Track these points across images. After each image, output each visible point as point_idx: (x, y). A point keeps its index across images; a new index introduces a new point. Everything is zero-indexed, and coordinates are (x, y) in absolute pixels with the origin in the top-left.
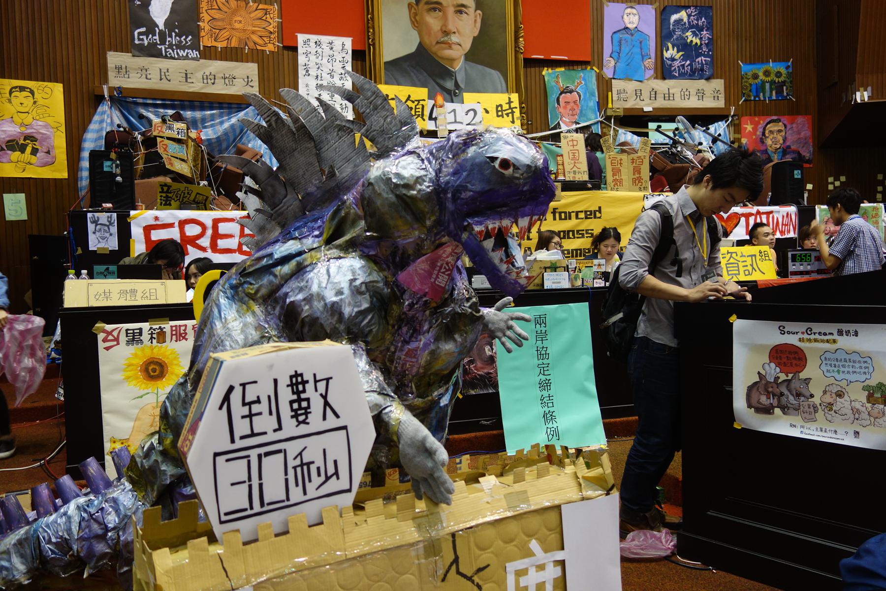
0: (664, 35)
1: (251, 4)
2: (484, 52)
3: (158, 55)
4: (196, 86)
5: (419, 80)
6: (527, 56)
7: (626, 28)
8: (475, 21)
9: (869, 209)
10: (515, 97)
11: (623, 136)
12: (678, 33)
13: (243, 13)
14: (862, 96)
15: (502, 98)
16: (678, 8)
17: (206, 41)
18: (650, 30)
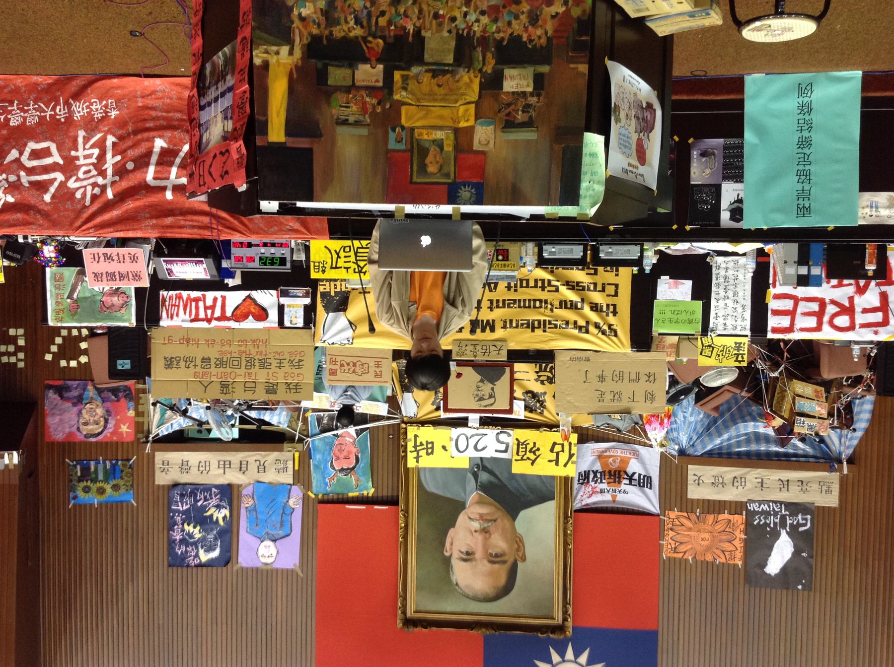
0: (227, 536)
1: (690, 558)
3: (790, 506)
4: (753, 475)
5: (517, 481)
6: (393, 508)
7: (274, 541)
8: (452, 544)
9: (67, 319)
10: (411, 463)
11: (282, 421)
12: (211, 537)
13: (699, 548)
15: (426, 462)
16: (210, 564)
17: (739, 519)
18: (245, 538)
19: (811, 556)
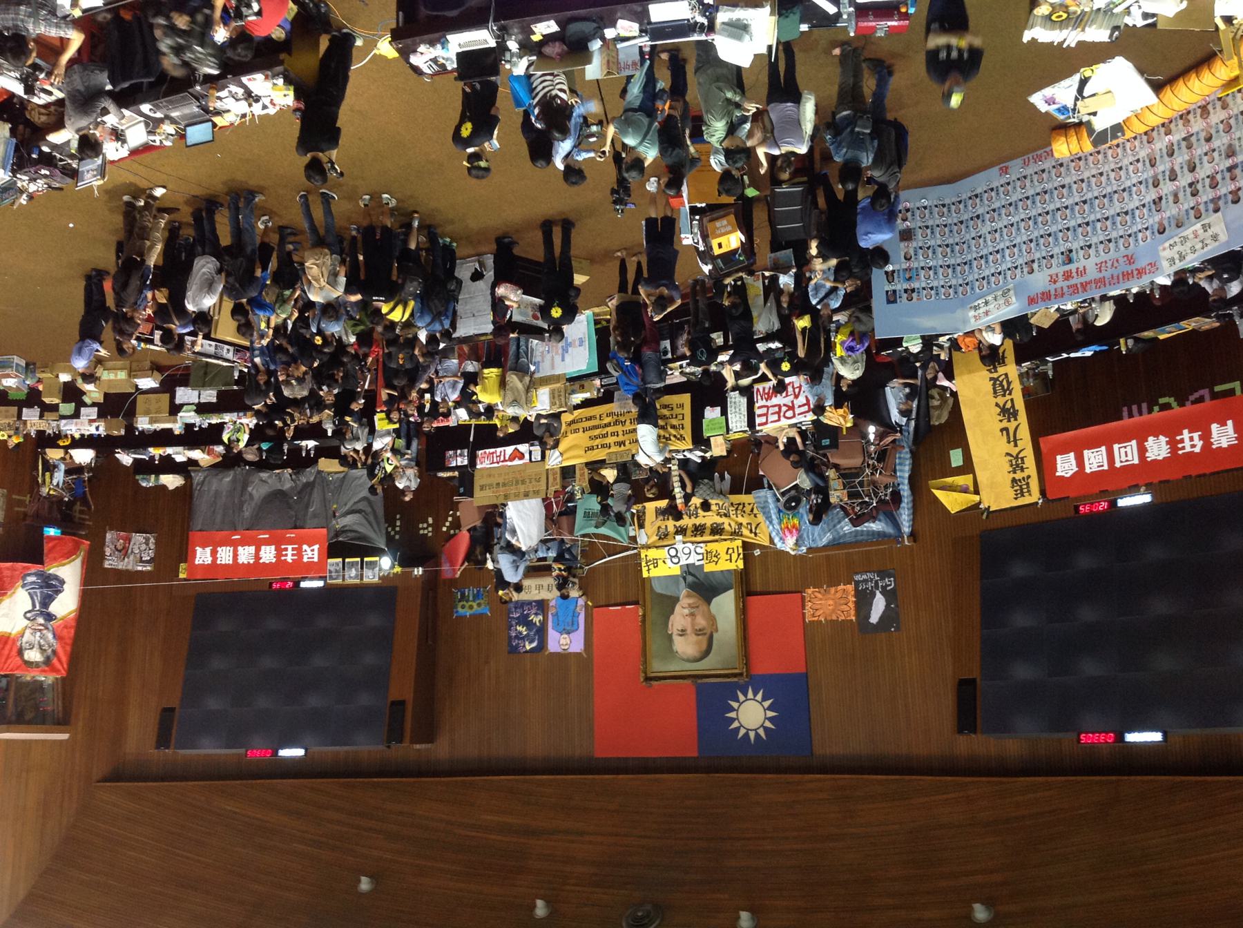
0: (541, 632)
2: (669, 603)
7: (568, 633)
10: (645, 575)
14: (418, 571)
15: (655, 573)
16: (532, 650)
19: (897, 606)
